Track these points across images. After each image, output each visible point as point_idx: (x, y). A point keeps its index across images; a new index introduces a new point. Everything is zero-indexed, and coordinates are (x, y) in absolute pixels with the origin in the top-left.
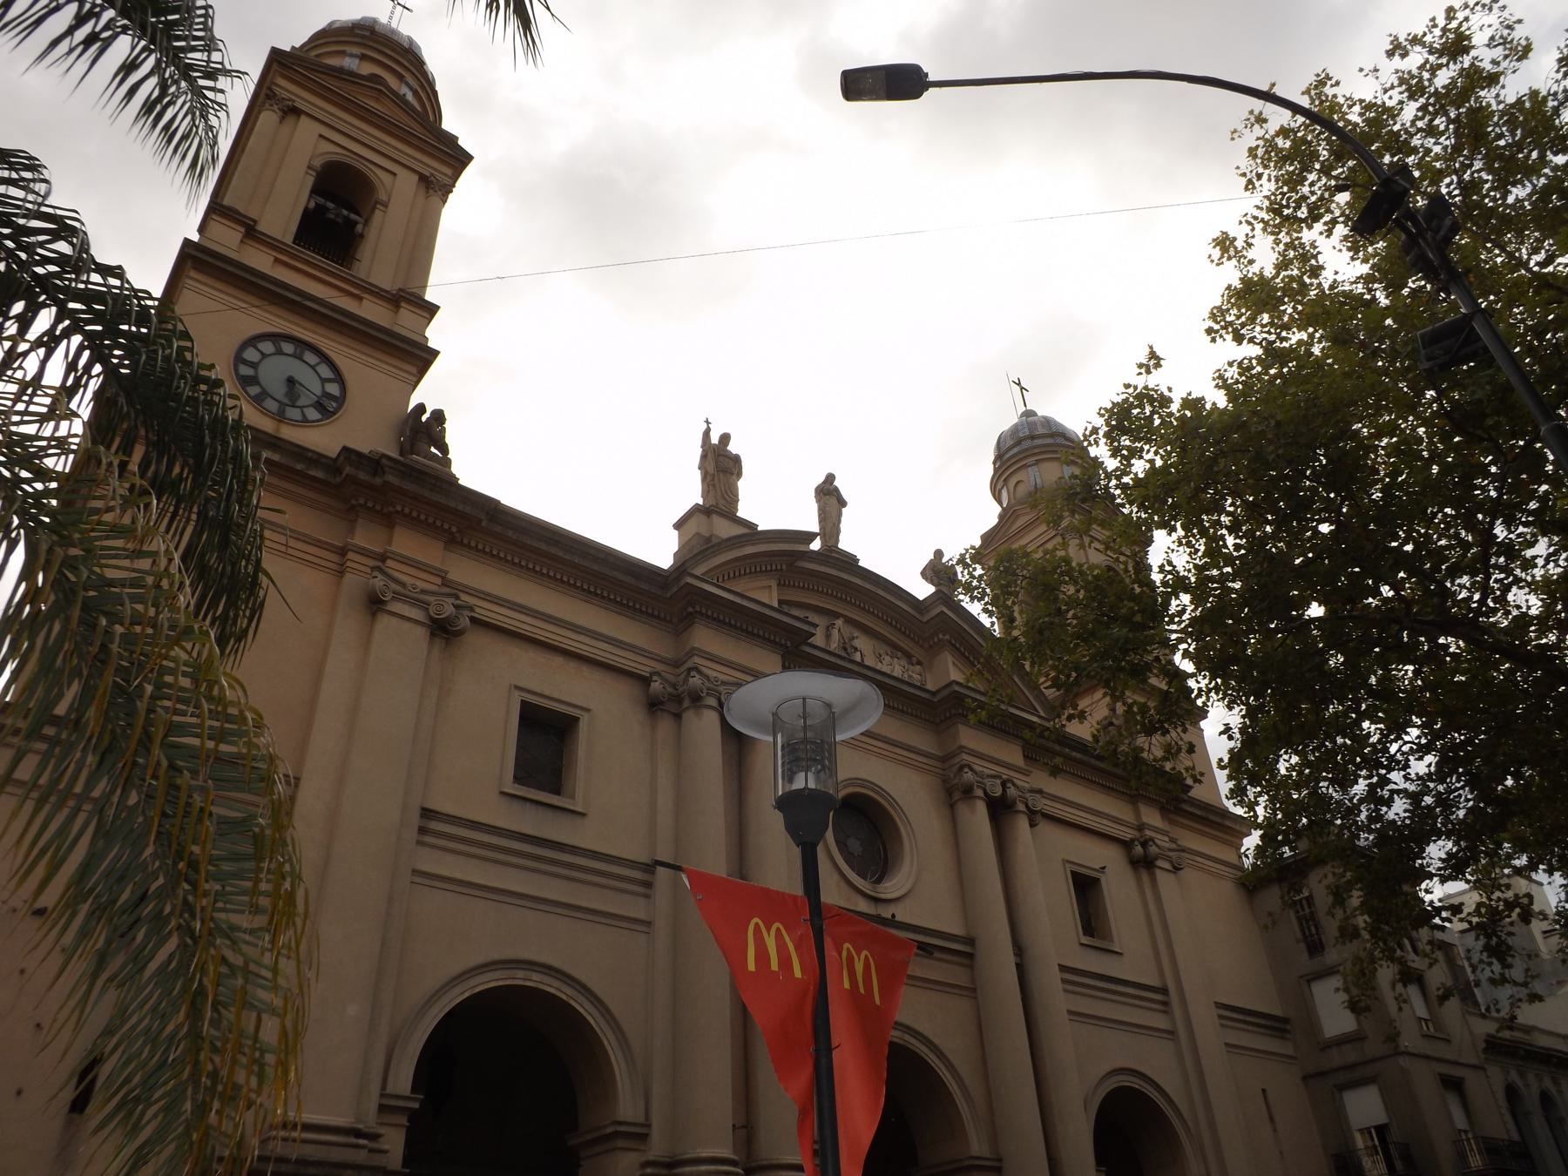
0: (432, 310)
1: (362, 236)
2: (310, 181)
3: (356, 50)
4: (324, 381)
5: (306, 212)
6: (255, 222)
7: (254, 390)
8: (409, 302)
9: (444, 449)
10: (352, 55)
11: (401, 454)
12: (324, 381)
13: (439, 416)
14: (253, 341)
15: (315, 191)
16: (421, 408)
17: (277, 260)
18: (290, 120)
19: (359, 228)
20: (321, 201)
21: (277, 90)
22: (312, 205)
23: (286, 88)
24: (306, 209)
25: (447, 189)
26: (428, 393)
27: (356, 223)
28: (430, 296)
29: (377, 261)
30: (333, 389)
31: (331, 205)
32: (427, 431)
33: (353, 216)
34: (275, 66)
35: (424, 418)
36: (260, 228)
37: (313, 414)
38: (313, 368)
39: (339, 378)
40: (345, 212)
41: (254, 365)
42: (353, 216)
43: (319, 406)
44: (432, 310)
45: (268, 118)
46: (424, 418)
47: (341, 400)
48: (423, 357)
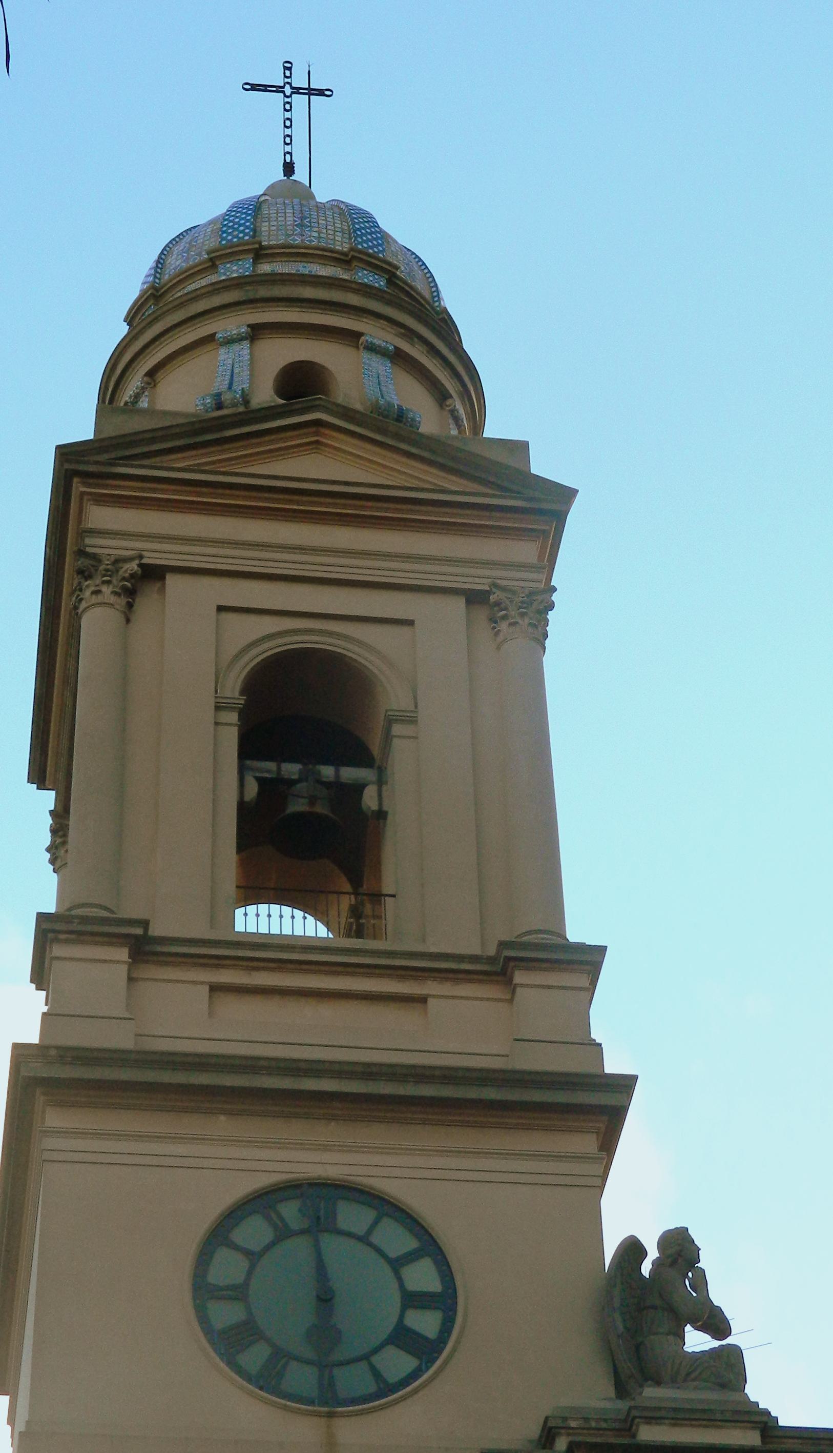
0: (589, 960)
1: (381, 815)
2: (231, 738)
3: (233, 324)
4: (397, 1264)
5: (247, 814)
6: (145, 924)
7: (255, 1357)
8: (529, 964)
9: (716, 1324)
10: (229, 341)
11: (621, 1390)
12: (397, 1264)
13: (680, 1249)
14: (219, 1234)
15: (251, 747)
16: (632, 1250)
17: (215, 989)
18: (147, 604)
19: (369, 799)
20: (269, 767)
21: (94, 544)
22: (252, 790)
23: (122, 528)
24: (242, 806)
25: (537, 605)
26: (637, 1200)
27: (358, 788)
28: (578, 930)
29: (428, 888)
30: (423, 1277)
31: (292, 769)
32: (659, 1294)
33: (349, 774)
34: (78, 487)
35: (646, 1268)
36: (156, 931)
37: (396, 1363)
38: (364, 1239)
39: (430, 1246)
40: (327, 772)
41: (238, 1293)
42: (349, 774)
43: (403, 1337)
44: (589, 960)
45: (97, 623)
46: (646, 1268)
47: (446, 1301)
48: (594, 1107)
